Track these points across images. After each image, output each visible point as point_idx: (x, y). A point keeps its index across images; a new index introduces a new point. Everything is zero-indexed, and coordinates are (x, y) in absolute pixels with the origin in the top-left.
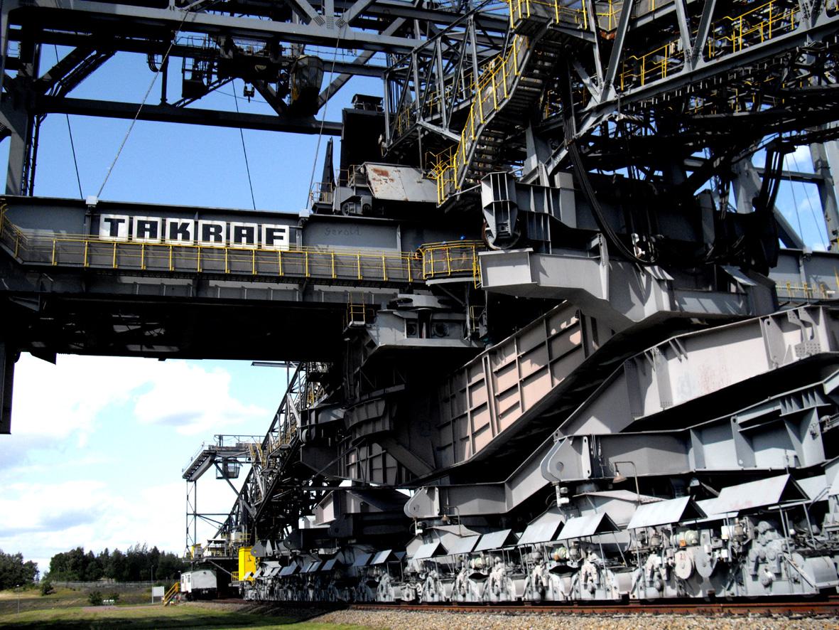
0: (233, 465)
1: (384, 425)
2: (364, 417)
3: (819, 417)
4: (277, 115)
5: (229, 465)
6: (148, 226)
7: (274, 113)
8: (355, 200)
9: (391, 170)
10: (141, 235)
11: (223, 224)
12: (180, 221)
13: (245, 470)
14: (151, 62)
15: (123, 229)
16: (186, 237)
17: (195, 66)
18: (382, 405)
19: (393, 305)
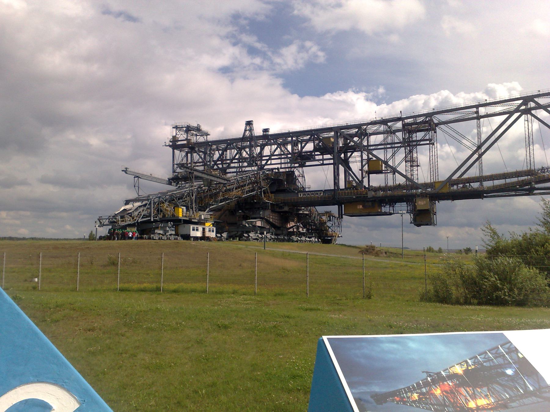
11: (314, 193)
12: (308, 193)
15: (301, 195)
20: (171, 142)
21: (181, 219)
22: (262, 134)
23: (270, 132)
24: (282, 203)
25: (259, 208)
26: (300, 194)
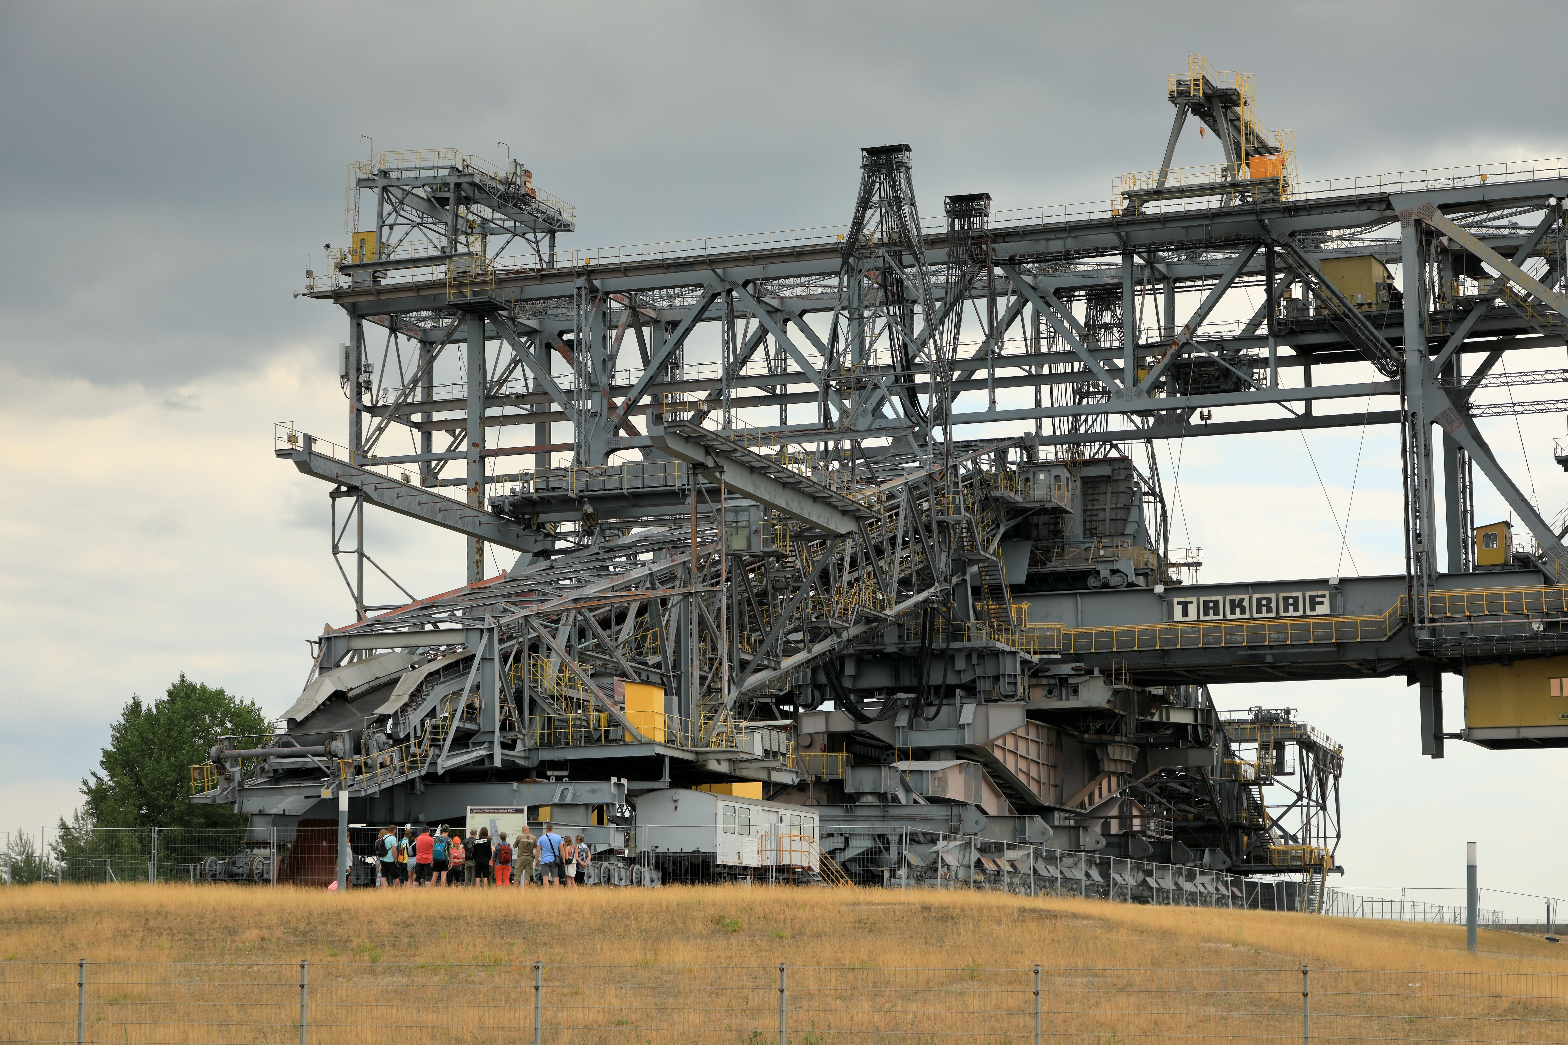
6: (1211, 605)
10: (1206, 614)
11: (1273, 596)
12: (1237, 598)
15: (1192, 609)
20: (343, 269)
21: (664, 756)
22: (944, 230)
23: (991, 218)
24: (1067, 658)
25: (949, 692)
26: (1185, 606)
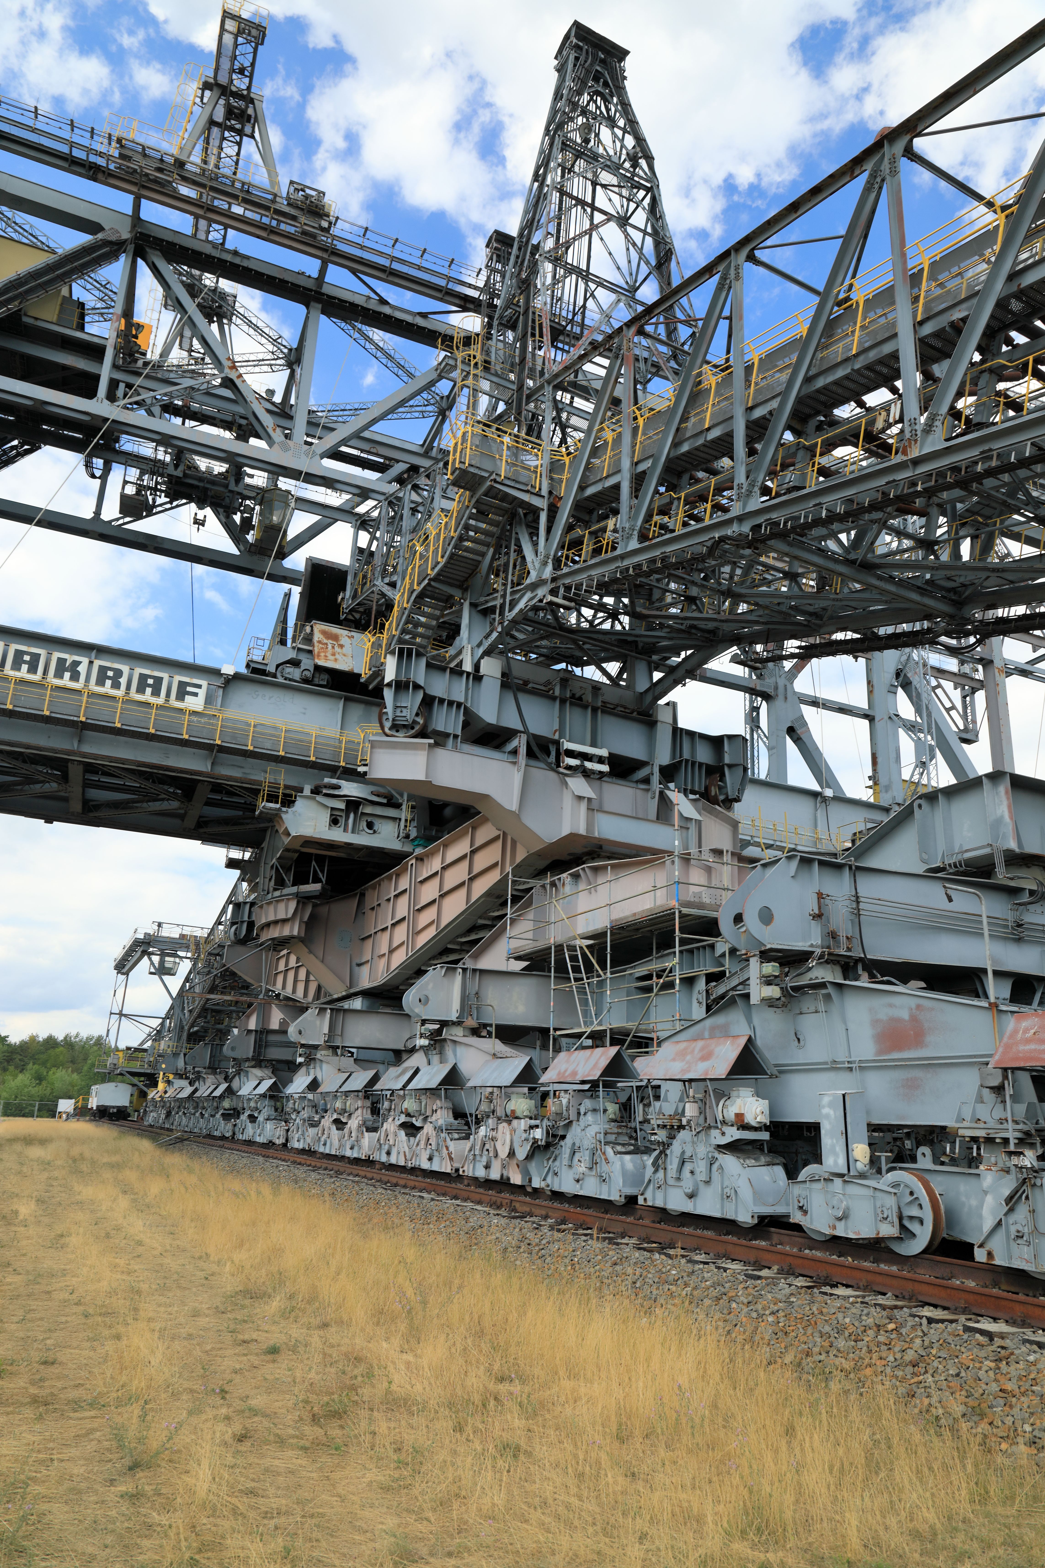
0: (172, 959)
1: (292, 930)
2: (271, 918)
3: (707, 983)
4: (238, 553)
5: (167, 959)
7: (236, 552)
8: (295, 663)
9: (342, 633)
11: (125, 669)
12: (70, 658)
13: (185, 967)
14: (88, 465)
16: (75, 677)
17: (140, 478)
18: (293, 905)
19: (316, 791)
